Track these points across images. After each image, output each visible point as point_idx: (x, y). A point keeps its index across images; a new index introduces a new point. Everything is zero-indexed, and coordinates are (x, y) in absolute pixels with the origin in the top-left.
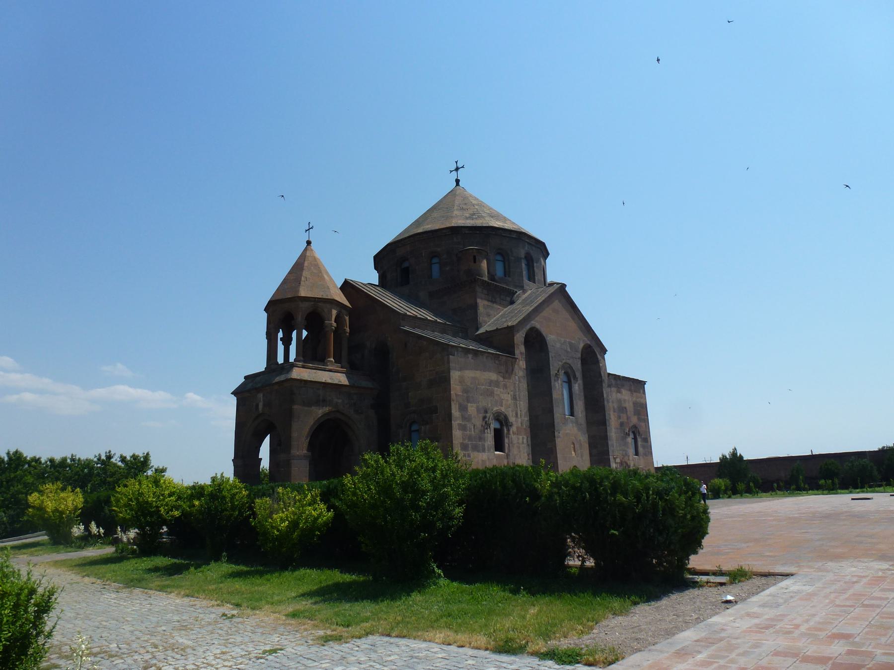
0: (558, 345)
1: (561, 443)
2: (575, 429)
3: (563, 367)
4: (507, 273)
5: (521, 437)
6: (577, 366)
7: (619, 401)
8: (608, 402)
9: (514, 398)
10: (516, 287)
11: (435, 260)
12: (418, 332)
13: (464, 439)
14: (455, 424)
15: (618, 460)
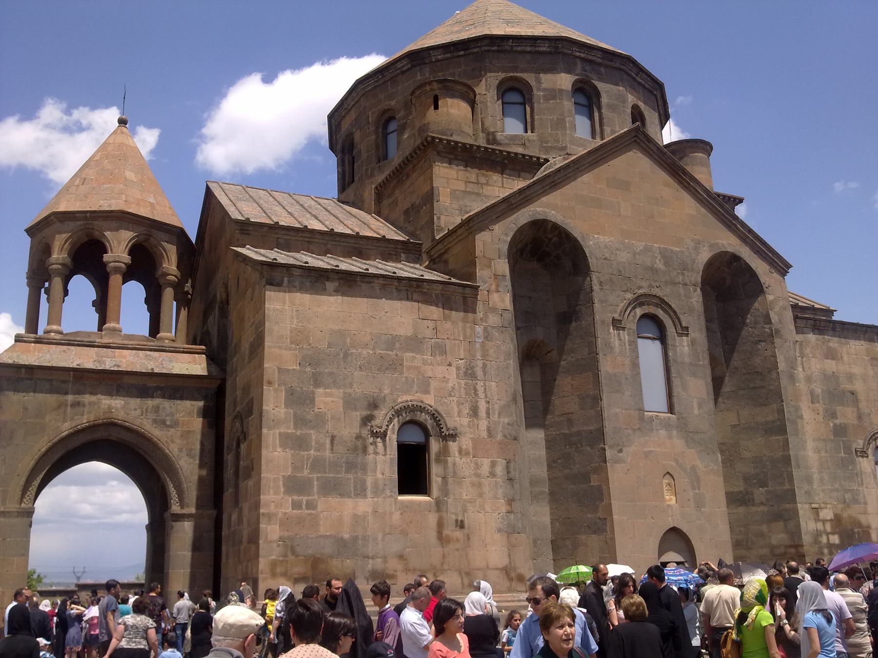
0: (624, 257)
1: (621, 475)
2: (679, 443)
3: (639, 301)
4: (529, 125)
5: (486, 463)
6: (691, 303)
7: (830, 378)
8: (792, 378)
9: (469, 373)
10: (547, 150)
11: (393, 126)
12: (282, 257)
13: (295, 468)
14: (270, 436)
15: (827, 514)
